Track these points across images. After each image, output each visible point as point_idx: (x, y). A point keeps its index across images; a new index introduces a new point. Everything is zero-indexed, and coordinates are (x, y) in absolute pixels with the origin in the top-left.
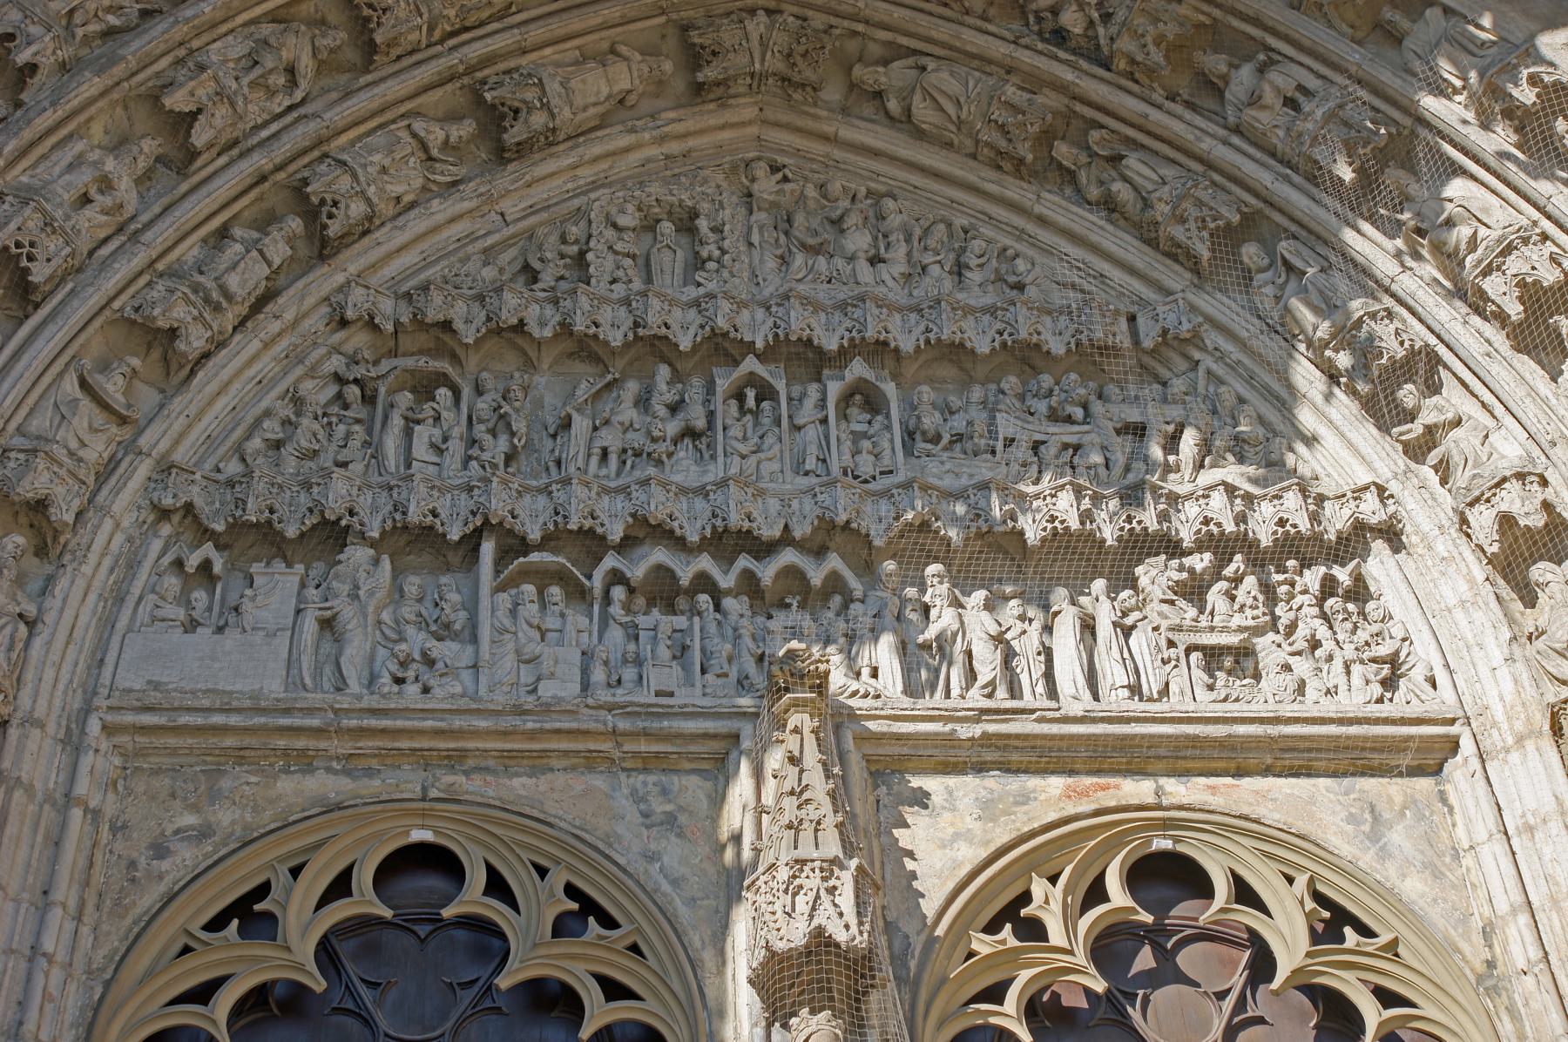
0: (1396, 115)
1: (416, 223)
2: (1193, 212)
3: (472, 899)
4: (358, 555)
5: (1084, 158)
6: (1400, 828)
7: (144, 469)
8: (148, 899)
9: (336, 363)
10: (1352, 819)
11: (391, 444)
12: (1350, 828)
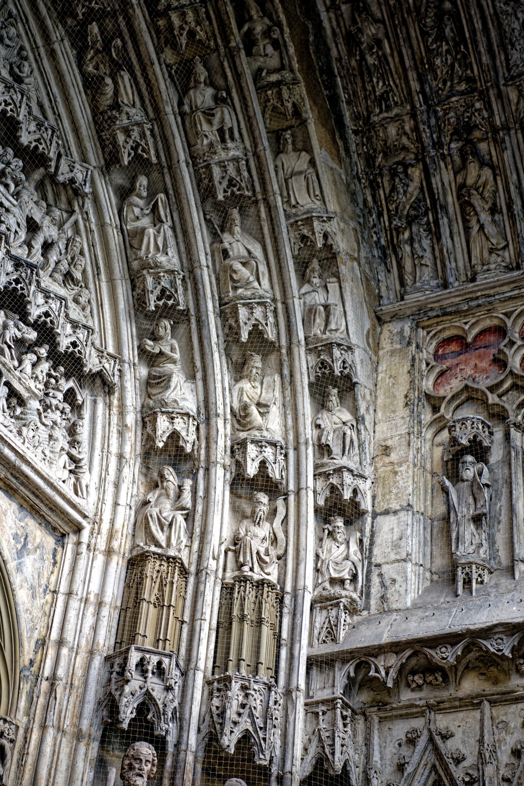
0: (258, 188)
2: (135, 134)
5: (99, 46)
6: (31, 557)
10: (16, 537)
12: (13, 542)
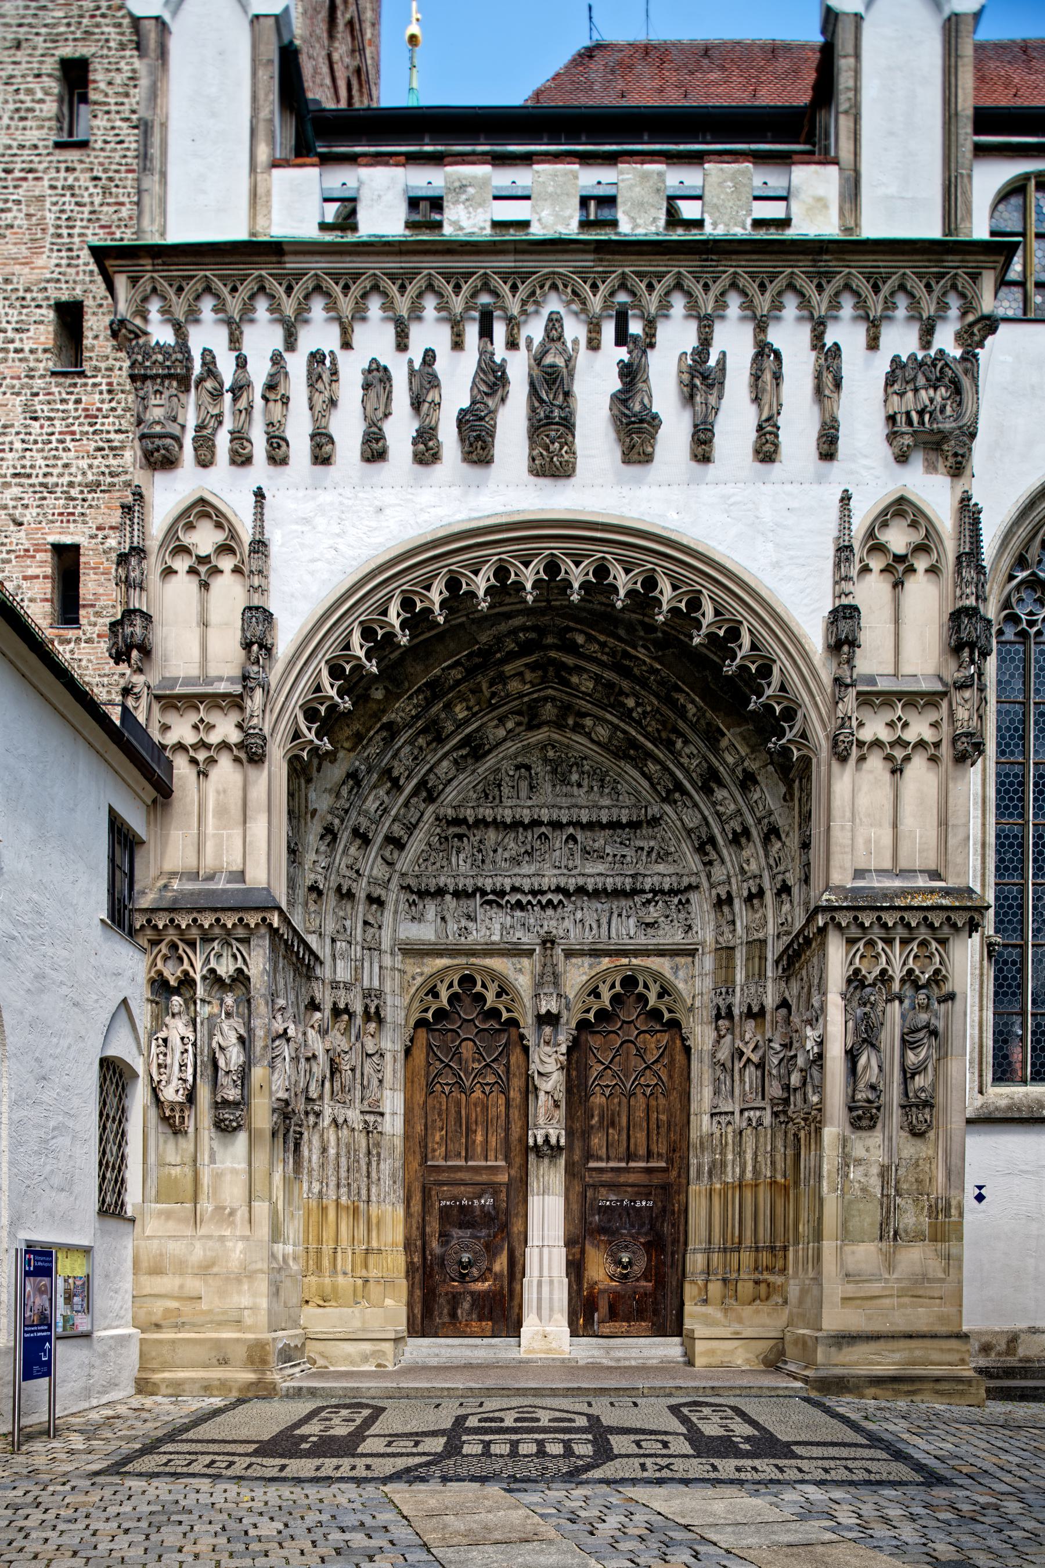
1: (455, 783)
3: (478, 988)
4: (448, 897)
7: (396, 876)
8: (413, 990)
9: (438, 830)
11: (454, 860)
